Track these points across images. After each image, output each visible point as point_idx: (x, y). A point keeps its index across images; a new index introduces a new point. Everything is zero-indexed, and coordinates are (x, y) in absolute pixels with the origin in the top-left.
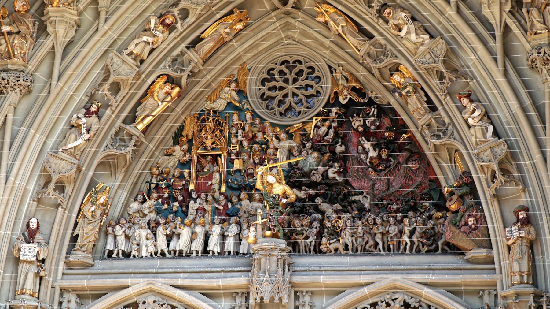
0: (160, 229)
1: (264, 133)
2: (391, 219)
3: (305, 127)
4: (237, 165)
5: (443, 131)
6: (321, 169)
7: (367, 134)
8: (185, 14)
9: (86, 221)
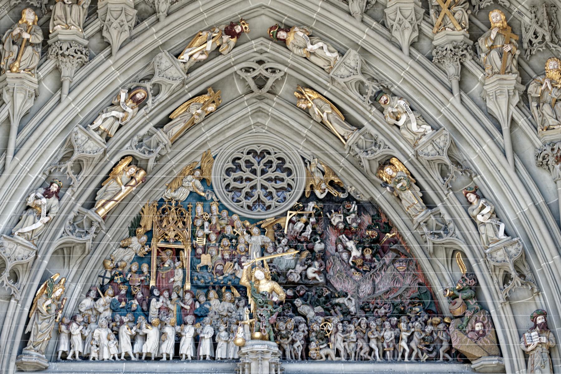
1: (233, 227)
2: (387, 323)
3: (278, 222)
4: (205, 260)
5: (443, 228)
6: (299, 268)
7: (347, 230)
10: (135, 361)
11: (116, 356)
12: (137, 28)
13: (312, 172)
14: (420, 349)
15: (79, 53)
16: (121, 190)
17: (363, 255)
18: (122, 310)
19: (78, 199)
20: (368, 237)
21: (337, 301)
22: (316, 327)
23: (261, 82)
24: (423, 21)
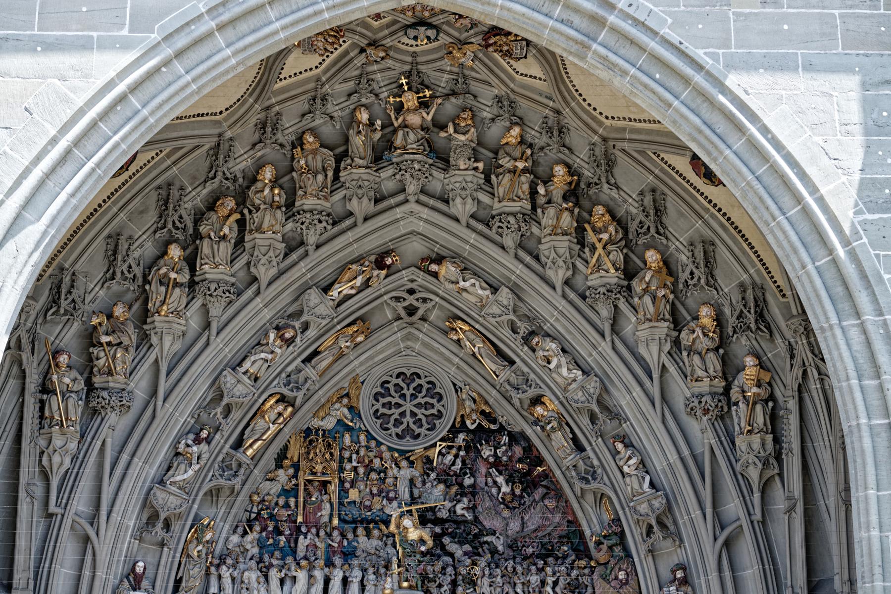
1: (382, 459)
2: (533, 568)
4: (353, 495)
6: (448, 505)
7: (497, 463)
8: (306, 327)
13: (463, 400)
17: (512, 490)
21: (485, 539)
22: (463, 571)
23: (411, 311)
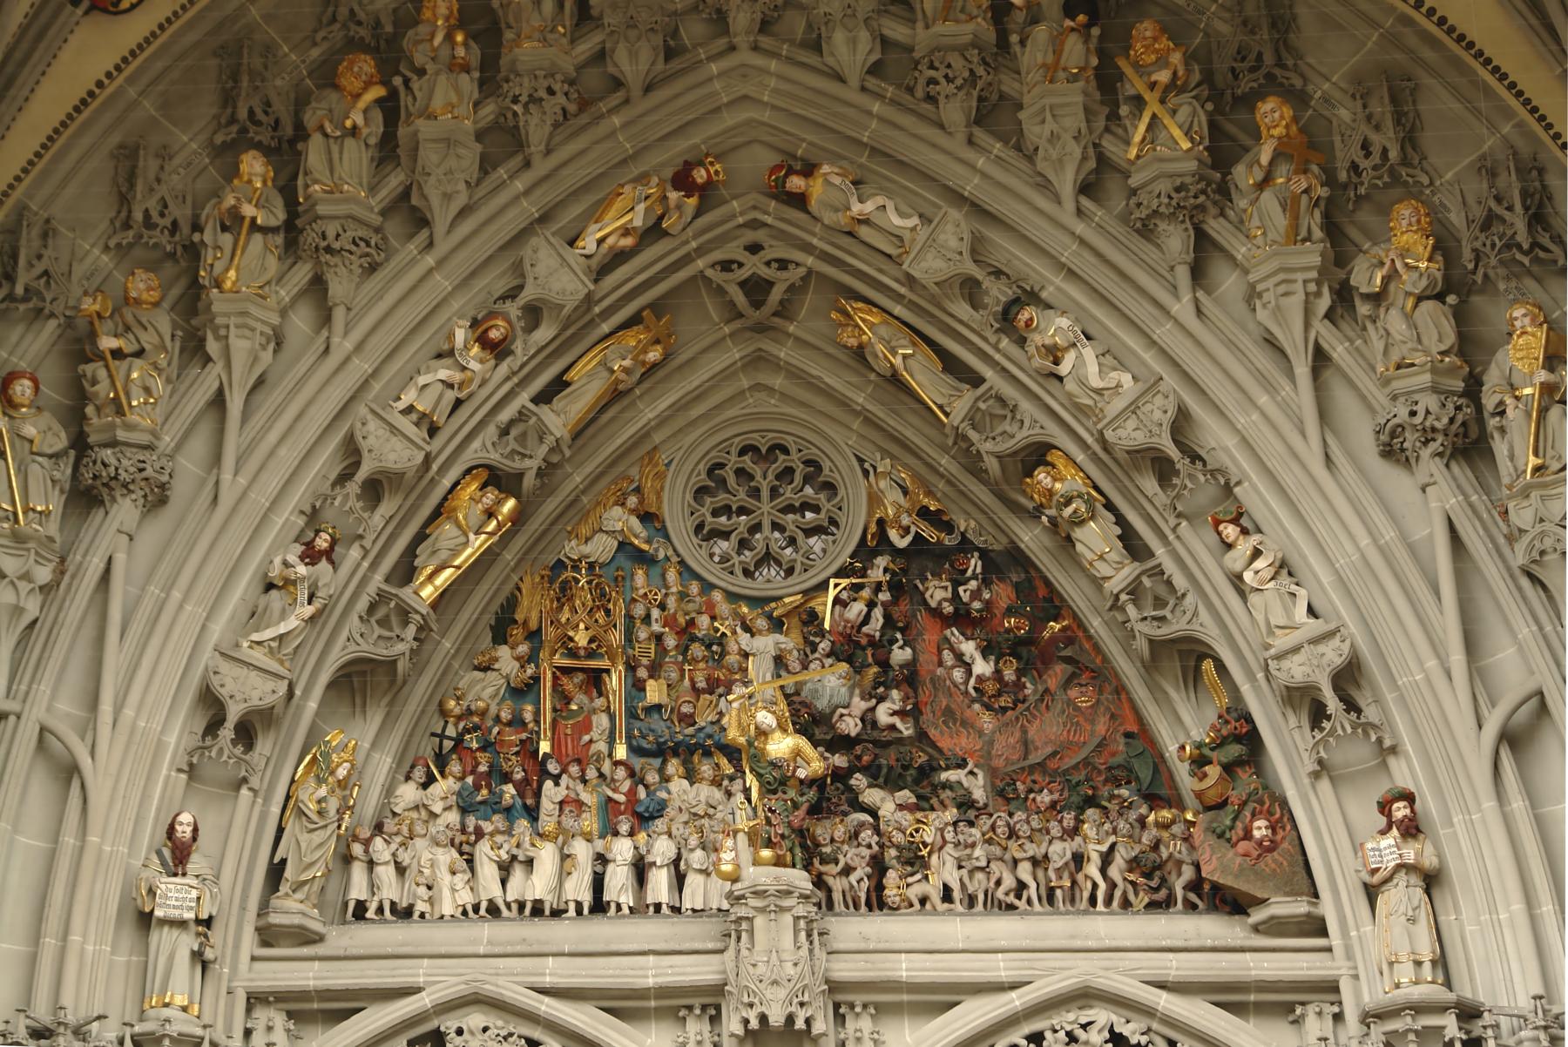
0: (483, 849)
9: (306, 823)
10: (509, 919)
11: (469, 908)
12: (484, 184)
14: (1133, 883)
15: (362, 244)
16: (466, 544)
18: (482, 808)
19: (374, 566)
20: (1008, 631)
24: (1107, 136)
